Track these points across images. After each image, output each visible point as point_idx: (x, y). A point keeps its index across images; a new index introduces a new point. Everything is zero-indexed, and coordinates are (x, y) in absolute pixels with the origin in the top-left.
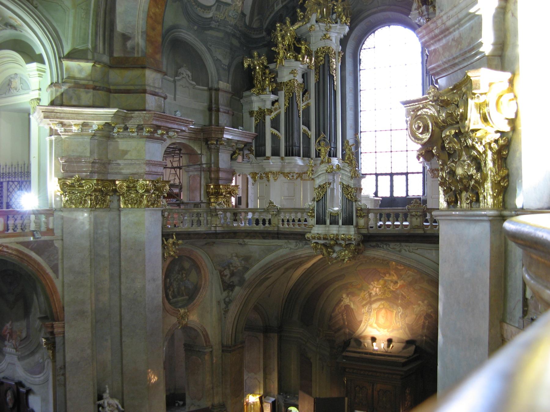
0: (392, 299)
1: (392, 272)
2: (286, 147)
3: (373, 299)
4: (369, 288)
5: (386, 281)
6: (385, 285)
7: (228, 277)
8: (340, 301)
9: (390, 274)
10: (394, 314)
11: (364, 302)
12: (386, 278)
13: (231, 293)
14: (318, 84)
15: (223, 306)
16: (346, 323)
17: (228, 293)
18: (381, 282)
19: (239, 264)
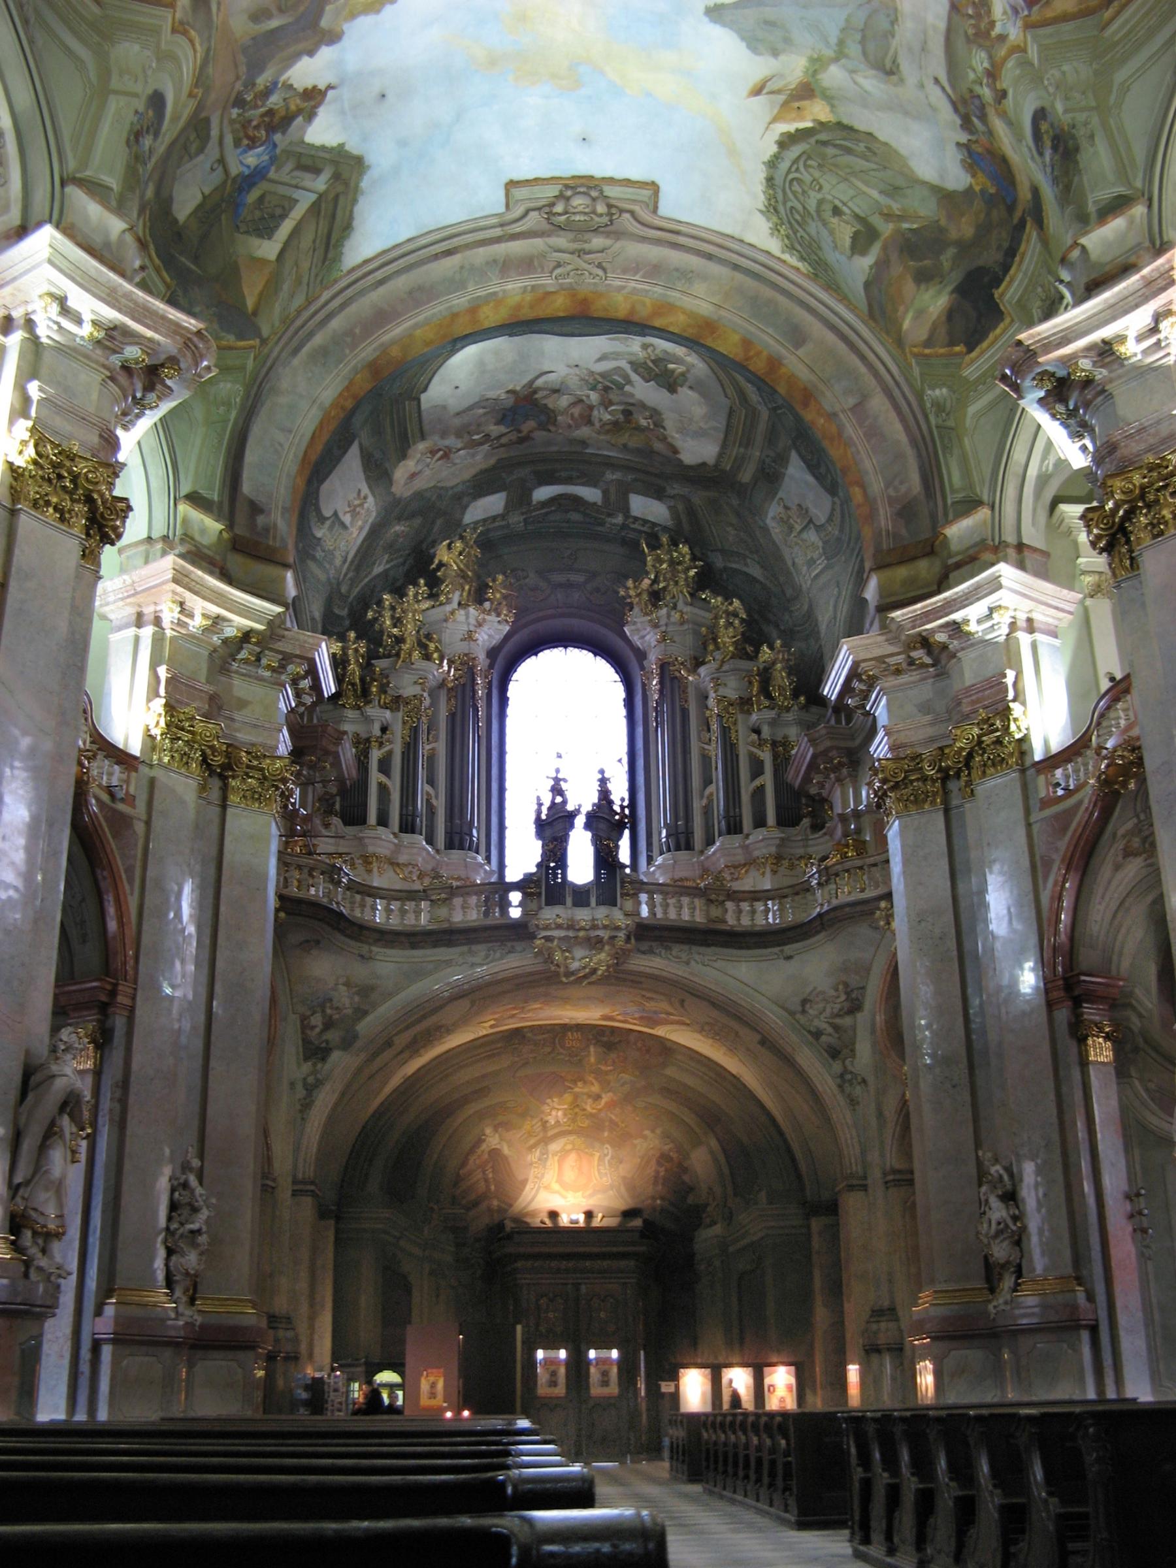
0: (590, 1130)
1: (590, 1078)
2: (401, 815)
3: (550, 1133)
4: (543, 1112)
5: (576, 1097)
6: (575, 1104)
7: (318, 1030)
8: (480, 1141)
9: (585, 1082)
10: (596, 1158)
11: (532, 1141)
12: (577, 1090)
13: (319, 1065)
14: (452, 716)
15: (301, 1092)
16: (493, 1187)
17: (314, 1065)
18: (568, 1097)
19: (347, 1001)
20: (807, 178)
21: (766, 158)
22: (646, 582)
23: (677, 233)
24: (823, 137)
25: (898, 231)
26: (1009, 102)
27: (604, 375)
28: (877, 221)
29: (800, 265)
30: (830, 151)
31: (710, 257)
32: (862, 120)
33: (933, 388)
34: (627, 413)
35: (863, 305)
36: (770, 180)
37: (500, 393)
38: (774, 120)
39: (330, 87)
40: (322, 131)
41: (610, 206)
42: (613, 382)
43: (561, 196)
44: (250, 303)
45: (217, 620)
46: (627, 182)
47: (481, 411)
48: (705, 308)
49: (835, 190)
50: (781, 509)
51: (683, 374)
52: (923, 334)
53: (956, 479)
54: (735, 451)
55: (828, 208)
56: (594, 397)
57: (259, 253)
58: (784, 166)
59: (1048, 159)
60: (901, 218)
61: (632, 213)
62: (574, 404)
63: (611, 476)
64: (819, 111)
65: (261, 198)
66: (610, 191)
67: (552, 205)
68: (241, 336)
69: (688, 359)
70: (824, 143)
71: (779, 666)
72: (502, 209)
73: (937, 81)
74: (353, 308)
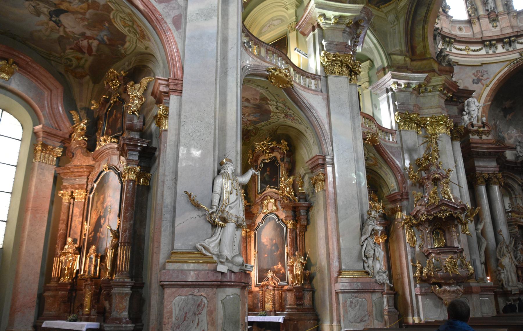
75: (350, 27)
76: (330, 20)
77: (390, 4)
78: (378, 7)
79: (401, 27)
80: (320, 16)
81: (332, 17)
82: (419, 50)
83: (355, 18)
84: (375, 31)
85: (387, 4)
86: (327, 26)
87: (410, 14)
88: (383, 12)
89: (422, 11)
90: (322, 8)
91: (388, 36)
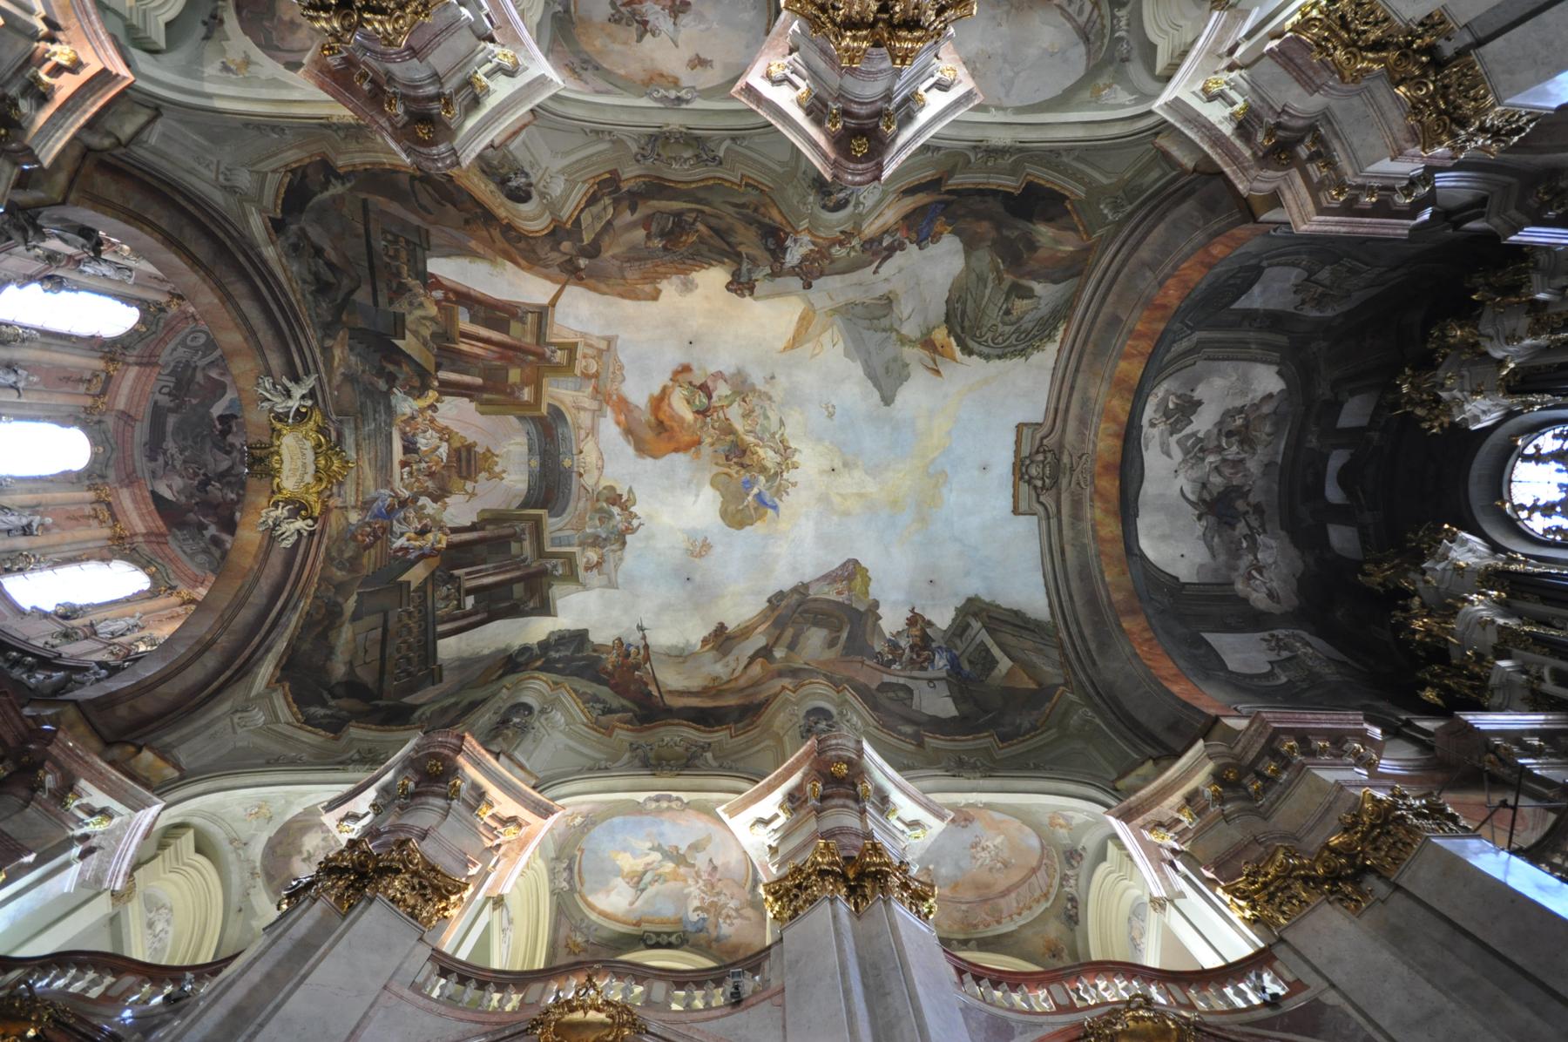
20: (989, 335)
21: (983, 361)
22: (1420, 412)
23: (1056, 410)
24: (959, 330)
25: (1007, 271)
26: (848, 227)
27: (1186, 452)
28: (1006, 286)
29: (1061, 329)
30: (967, 324)
31: (1072, 388)
32: (938, 309)
33: (1106, 217)
34: (1229, 434)
35: (1072, 283)
36: (999, 357)
37: (1199, 528)
38: (954, 360)
39: (912, 610)
40: (942, 618)
41: (1038, 452)
42: (1194, 445)
43: (1029, 482)
44: (1033, 686)
45: (1190, 799)
46: (1018, 442)
47: (1216, 540)
48: (1104, 388)
49: (993, 315)
50: (1307, 307)
51: (1178, 397)
52: (1070, 235)
53: (1155, 174)
54: (1255, 350)
55: (1006, 319)
56: (1211, 458)
57: (1004, 671)
58: (986, 350)
59: (842, 195)
60: (998, 270)
61: (1042, 439)
62: (1220, 473)
63: (1313, 441)
64: (940, 335)
65: (970, 662)
66: (1025, 451)
67: (1035, 487)
68: (1050, 698)
69: (1160, 395)
70: (963, 328)
71: (1492, 280)
72: (1035, 518)
73: (875, 272)
74: (1082, 619)
75: (431, 99)
76: (488, 75)
77: (277, 196)
78: (293, 171)
79: (203, 182)
80: (516, 64)
81: (492, 85)
82: (105, 185)
83: (449, 128)
84: (246, 125)
85: (283, 190)
86: (481, 56)
87: (213, 219)
88: (274, 171)
89: (202, 250)
90: (529, 84)
91: (206, 143)
